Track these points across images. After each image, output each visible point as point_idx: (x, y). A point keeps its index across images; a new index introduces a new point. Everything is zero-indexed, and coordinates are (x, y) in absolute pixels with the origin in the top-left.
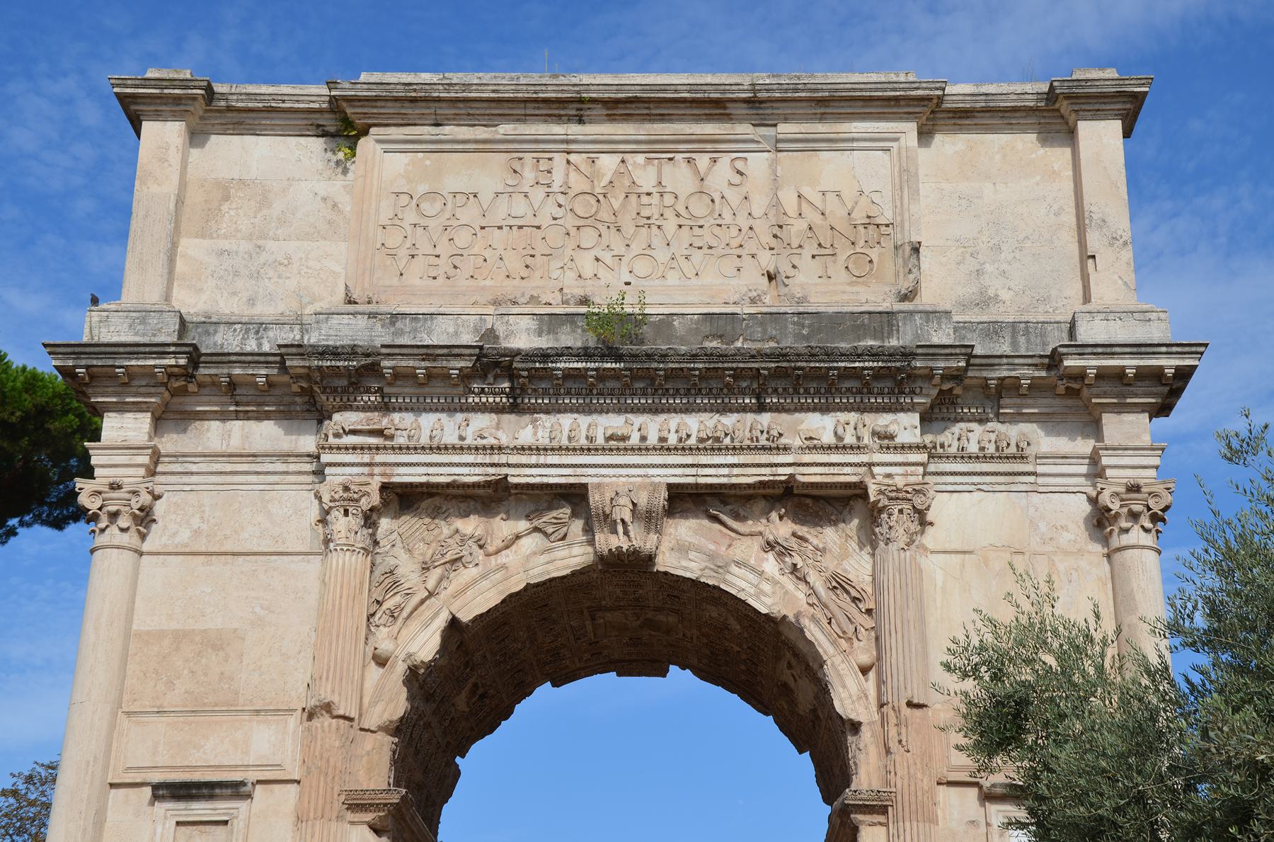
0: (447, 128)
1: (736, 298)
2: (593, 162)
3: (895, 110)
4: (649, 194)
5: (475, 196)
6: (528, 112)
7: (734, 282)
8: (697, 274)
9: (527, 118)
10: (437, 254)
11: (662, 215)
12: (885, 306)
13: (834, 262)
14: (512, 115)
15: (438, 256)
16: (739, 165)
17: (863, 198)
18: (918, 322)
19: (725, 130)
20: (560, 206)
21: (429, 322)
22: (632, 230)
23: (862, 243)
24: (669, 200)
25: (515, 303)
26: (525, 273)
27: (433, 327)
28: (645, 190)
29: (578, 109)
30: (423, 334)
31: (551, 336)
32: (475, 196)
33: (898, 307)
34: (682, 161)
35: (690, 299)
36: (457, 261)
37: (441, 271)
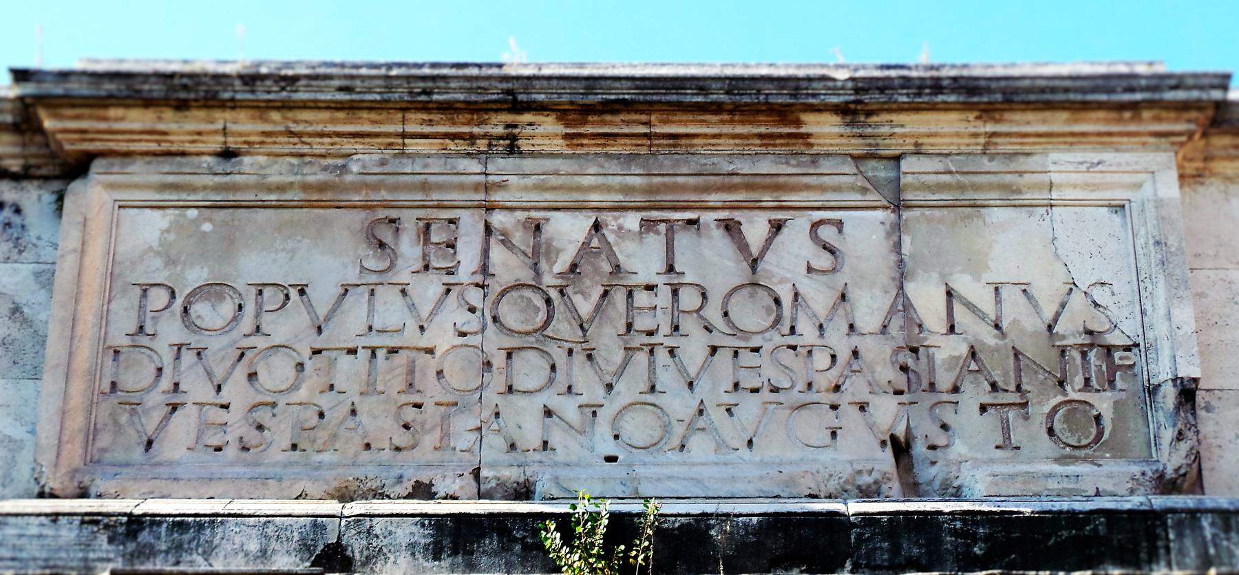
0: (247, 160)
1: (833, 486)
2: (538, 228)
3: (1132, 128)
4: (650, 288)
5: (302, 292)
6: (410, 128)
7: (826, 456)
8: (750, 442)
9: (407, 141)
10: (224, 402)
11: (676, 328)
12: (1134, 502)
13: (1026, 417)
14: (377, 135)
15: (225, 407)
16: (827, 233)
17: (1077, 298)
18: (1208, 532)
19: (798, 165)
20: (472, 310)
21: (208, 531)
22: (619, 356)
23: (1079, 381)
24: (689, 299)
25: (383, 496)
26: (402, 438)
27: (216, 541)
28: (642, 279)
29: (508, 126)
30: (195, 556)
31: (460, 559)
32: (302, 292)
33: (1160, 502)
34: (713, 225)
35: (739, 488)
36: (264, 416)
37: (232, 436)
